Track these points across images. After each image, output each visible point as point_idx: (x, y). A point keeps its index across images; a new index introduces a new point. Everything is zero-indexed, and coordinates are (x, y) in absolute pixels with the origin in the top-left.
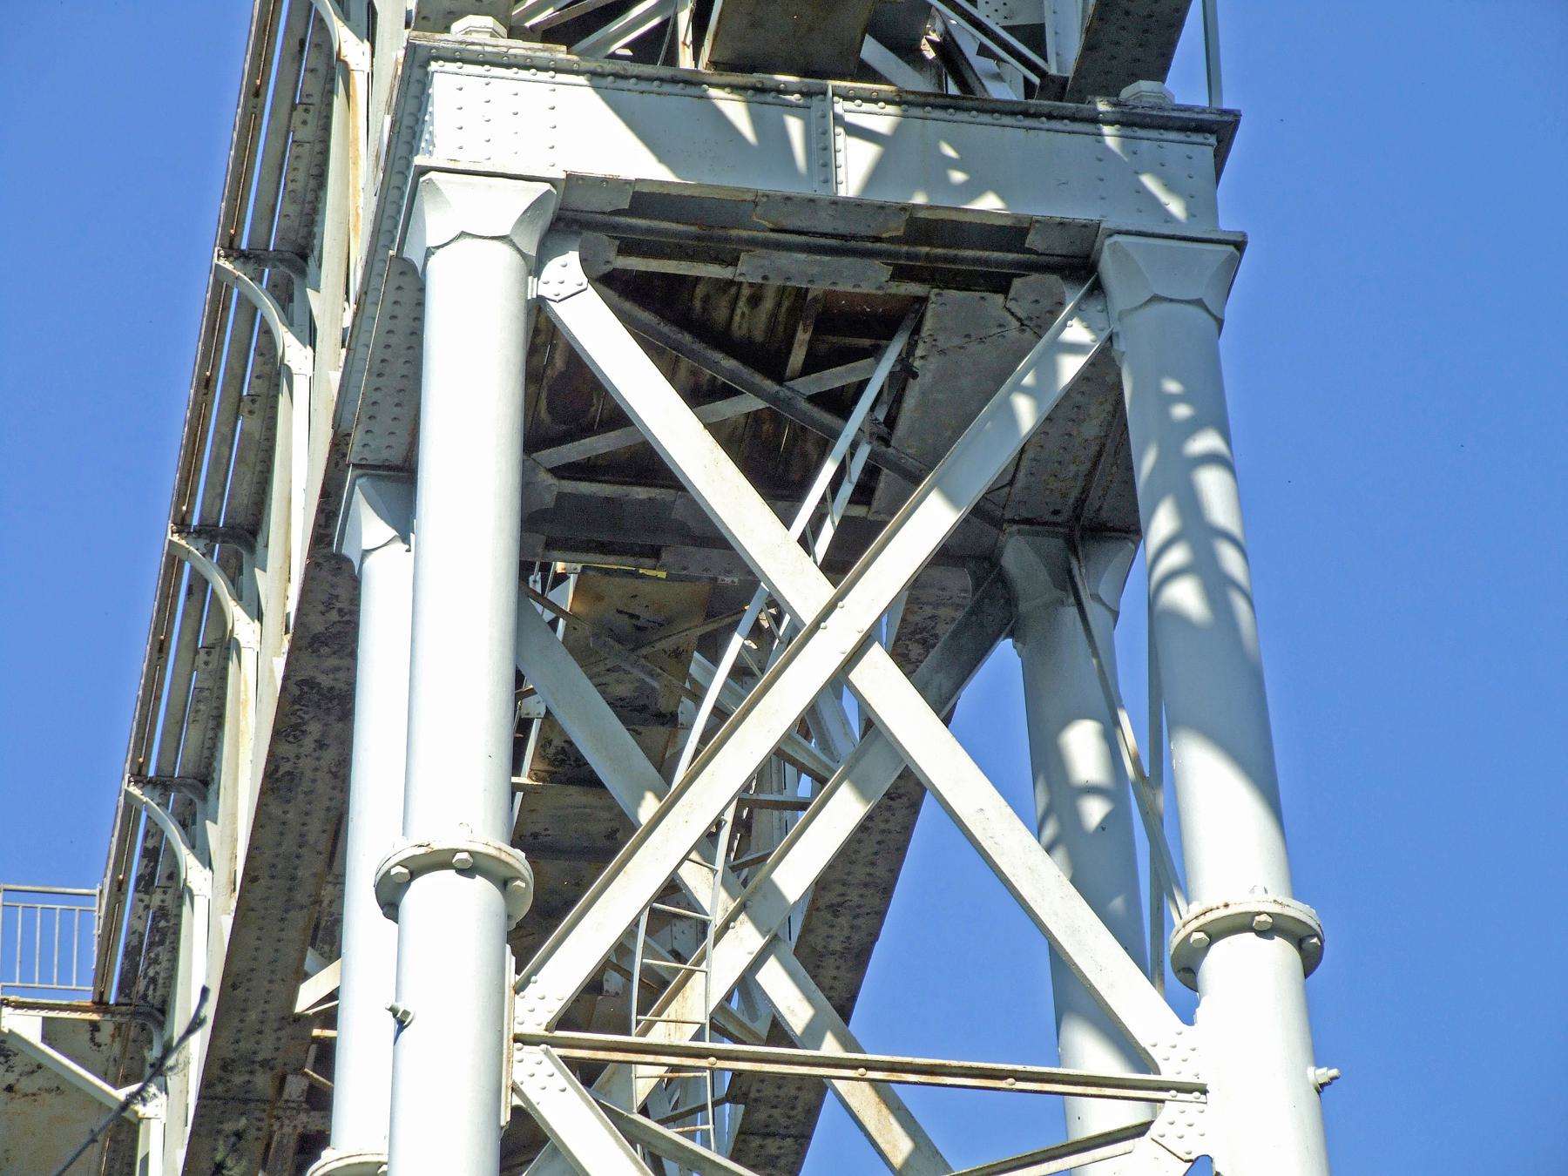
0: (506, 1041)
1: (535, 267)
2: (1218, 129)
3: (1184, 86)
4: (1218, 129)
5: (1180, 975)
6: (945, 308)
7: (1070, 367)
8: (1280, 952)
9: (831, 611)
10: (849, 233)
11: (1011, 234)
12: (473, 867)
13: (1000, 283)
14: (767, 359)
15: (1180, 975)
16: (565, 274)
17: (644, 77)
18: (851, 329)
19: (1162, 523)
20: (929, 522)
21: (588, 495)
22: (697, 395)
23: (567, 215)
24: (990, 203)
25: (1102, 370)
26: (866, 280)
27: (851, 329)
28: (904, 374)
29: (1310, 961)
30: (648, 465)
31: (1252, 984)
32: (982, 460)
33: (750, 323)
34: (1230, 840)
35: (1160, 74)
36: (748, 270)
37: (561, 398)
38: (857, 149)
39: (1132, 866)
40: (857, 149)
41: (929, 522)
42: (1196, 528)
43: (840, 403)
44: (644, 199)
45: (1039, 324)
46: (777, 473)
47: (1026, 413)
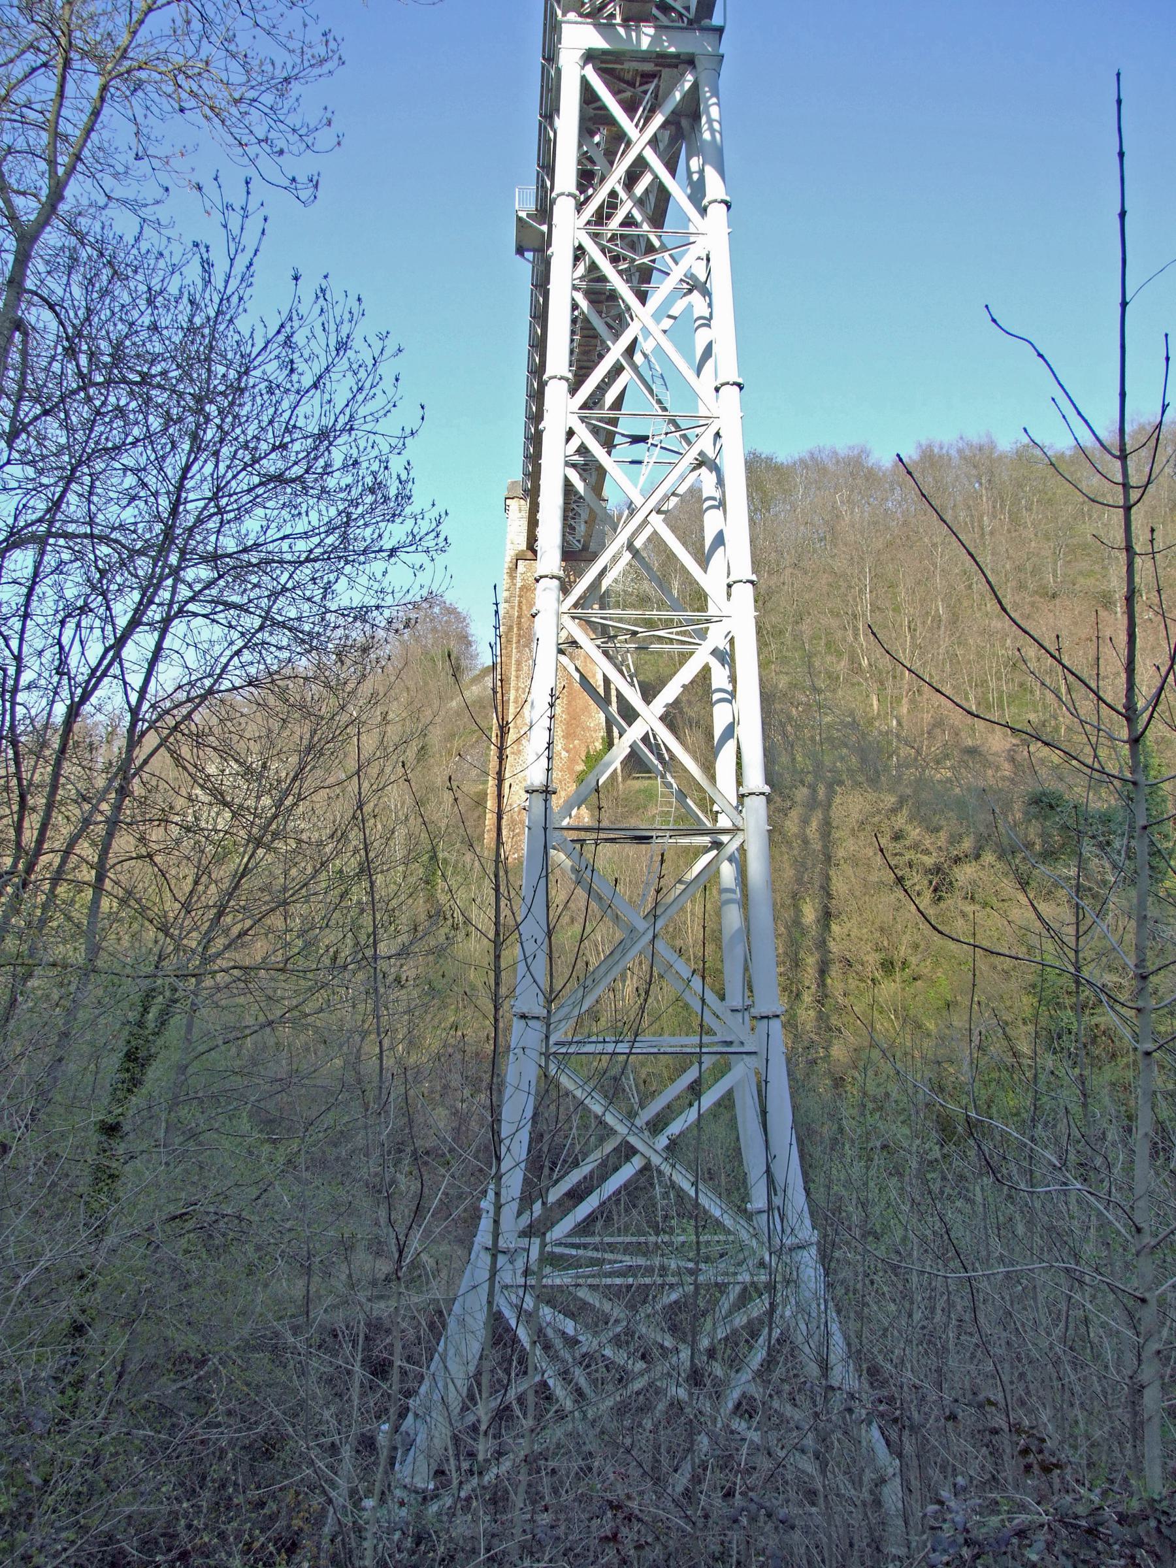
0: (559, 615)
1: (583, 68)
2: (720, 30)
3: (716, 20)
4: (720, 30)
5: (703, 211)
6: (666, 72)
7: (687, 85)
8: (724, 206)
9: (640, 137)
10: (644, 57)
11: (677, 56)
12: (569, 195)
13: (676, 66)
14: (632, 84)
15: (703, 211)
16: (589, 67)
17: (606, 29)
18: (647, 77)
19: (704, 119)
20: (659, 119)
21: (593, 116)
22: (615, 93)
23: (590, 56)
24: (672, 50)
25: (695, 86)
26: (649, 67)
27: (647, 77)
28: (657, 87)
29: (729, 207)
30: (604, 108)
31: (717, 212)
32: (669, 106)
33: (628, 77)
34: (715, 187)
35: (710, 18)
36: (626, 66)
37: (588, 96)
38: (645, 38)
39: (697, 192)
40: (645, 38)
41: (659, 119)
42: (710, 121)
43: (645, 92)
44: (604, 52)
45: (683, 75)
46: (630, 108)
47: (678, 96)
